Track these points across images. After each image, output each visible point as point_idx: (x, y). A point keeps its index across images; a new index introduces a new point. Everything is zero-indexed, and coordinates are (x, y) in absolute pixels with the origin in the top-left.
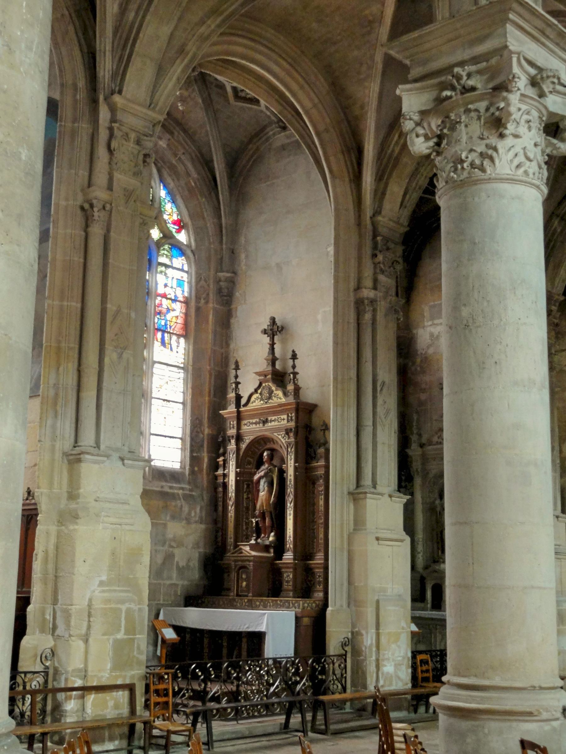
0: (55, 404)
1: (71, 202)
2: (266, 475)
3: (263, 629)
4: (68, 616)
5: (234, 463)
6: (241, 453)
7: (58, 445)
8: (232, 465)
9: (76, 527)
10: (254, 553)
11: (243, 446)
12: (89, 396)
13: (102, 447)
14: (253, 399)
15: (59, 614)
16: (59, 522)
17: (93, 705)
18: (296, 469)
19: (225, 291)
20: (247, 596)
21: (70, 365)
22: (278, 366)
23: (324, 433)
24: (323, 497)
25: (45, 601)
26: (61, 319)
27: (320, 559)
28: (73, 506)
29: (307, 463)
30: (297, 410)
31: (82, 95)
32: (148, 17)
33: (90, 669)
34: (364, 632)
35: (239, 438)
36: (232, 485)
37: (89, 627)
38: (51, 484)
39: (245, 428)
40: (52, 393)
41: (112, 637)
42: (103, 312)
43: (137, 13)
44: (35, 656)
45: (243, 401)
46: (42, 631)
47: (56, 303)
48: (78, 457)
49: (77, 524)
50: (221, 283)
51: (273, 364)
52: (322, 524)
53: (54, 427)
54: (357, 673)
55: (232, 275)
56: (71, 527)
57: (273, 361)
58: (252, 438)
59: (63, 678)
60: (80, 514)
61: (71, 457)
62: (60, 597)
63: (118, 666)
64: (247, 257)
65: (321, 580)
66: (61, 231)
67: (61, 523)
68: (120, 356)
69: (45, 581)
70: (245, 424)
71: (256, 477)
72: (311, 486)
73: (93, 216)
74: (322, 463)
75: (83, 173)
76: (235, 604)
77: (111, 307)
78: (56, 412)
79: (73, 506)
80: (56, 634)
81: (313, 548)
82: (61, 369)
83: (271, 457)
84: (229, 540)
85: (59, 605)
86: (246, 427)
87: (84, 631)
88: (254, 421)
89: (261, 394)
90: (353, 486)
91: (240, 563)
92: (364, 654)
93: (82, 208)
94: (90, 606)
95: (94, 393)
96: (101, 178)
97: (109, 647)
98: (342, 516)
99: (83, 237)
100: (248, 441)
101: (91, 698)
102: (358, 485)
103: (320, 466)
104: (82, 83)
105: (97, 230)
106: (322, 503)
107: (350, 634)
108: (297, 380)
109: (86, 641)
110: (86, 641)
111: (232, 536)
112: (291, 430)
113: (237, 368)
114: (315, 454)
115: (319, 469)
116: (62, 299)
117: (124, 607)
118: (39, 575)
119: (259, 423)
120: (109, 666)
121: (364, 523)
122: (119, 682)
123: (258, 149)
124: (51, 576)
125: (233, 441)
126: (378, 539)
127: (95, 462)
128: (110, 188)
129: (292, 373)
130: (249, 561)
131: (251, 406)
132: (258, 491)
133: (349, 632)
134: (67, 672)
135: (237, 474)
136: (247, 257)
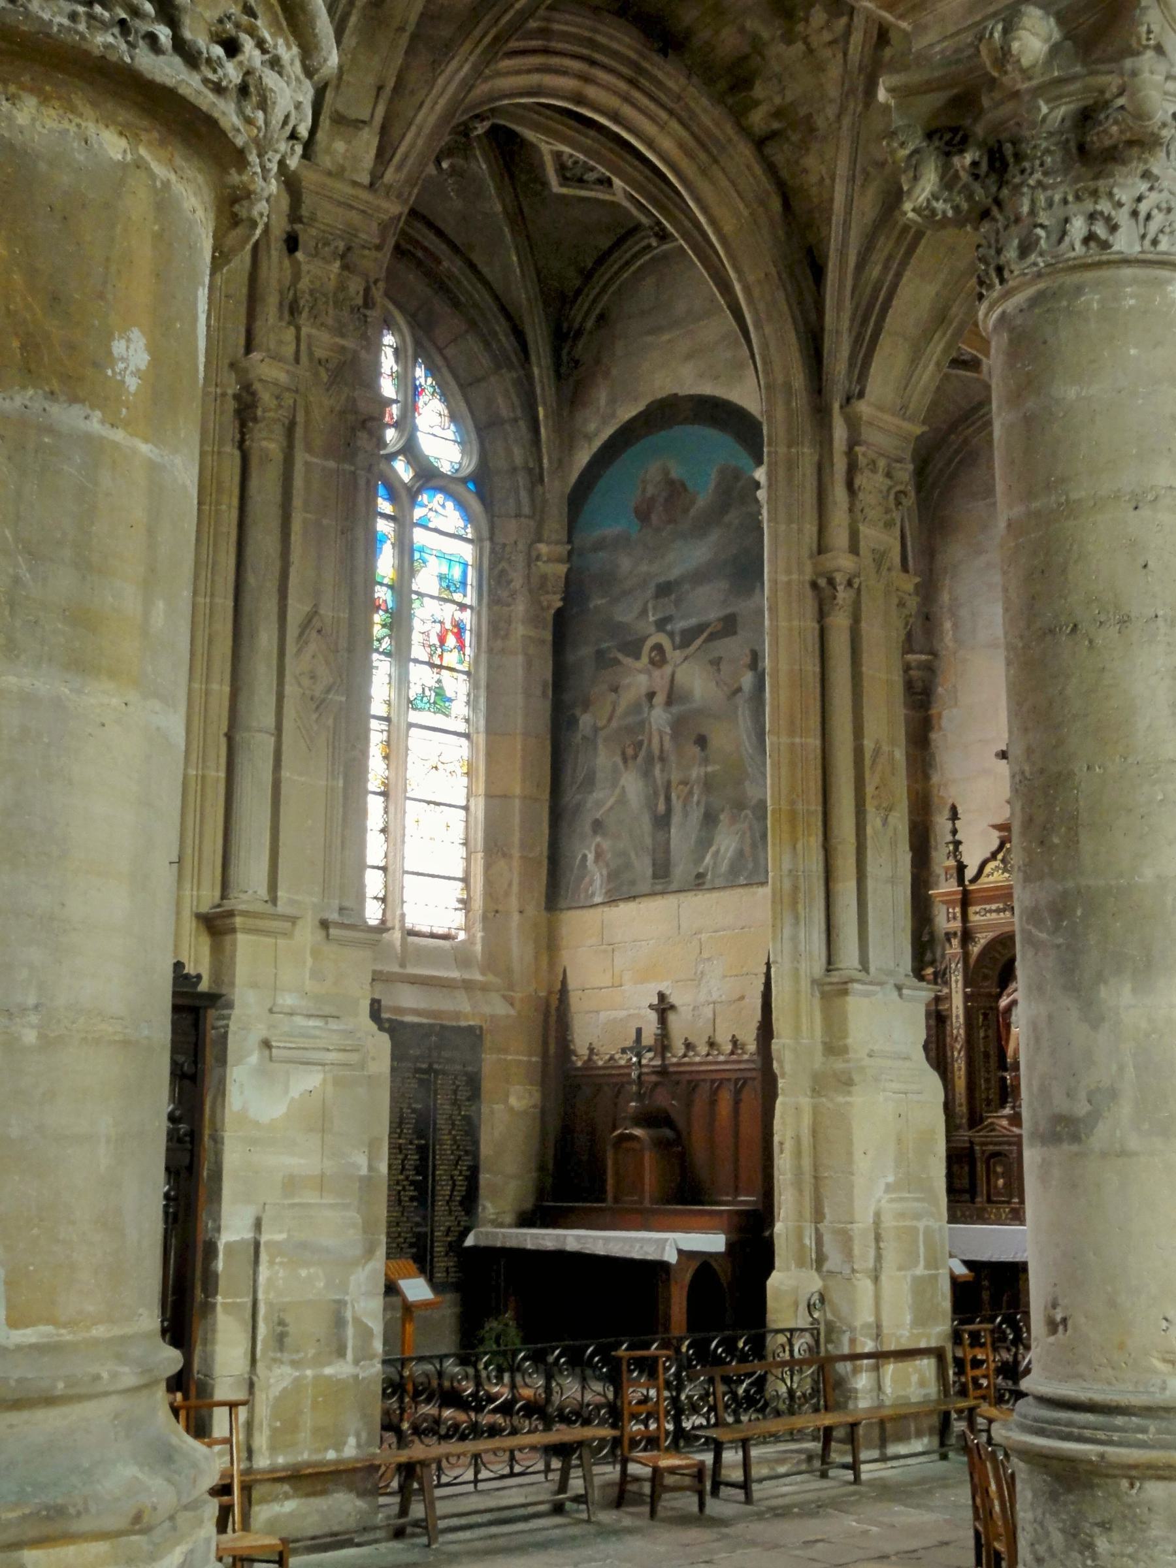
0: (794, 903)
1: (795, 577)
4: (846, 1240)
5: (960, 978)
6: (972, 960)
7: (803, 967)
8: (957, 982)
9: (848, 1099)
11: (975, 950)
12: (846, 890)
13: (872, 969)
15: (827, 1238)
16: (814, 1090)
17: (893, 1381)
19: (919, 685)
20: (1009, 1202)
21: (813, 839)
25: (800, 1215)
26: (792, 765)
28: (839, 1065)
31: (801, 402)
32: (908, 274)
33: (885, 1323)
35: (967, 936)
36: (957, 1017)
37: (879, 1258)
38: (797, 1029)
40: (787, 885)
41: (909, 1273)
42: (859, 752)
43: (886, 268)
44: (796, 1304)
45: (970, 873)
46: (801, 1264)
47: (785, 740)
48: (844, 986)
49: (849, 1093)
50: (912, 672)
53: (794, 939)
55: (930, 657)
56: (840, 1099)
58: (991, 935)
59: (845, 1339)
60: (856, 1078)
61: (827, 988)
62: (826, 1210)
63: (921, 1319)
64: (955, 626)
66: (783, 624)
67: (816, 1091)
68: (885, 822)
69: (798, 1183)
70: (976, 913)
73: (835, 598)
75: (811, 529)
76: (986, 1216)
77: (868, 744)
78: (797, 918)
79: (839, 1065)
80: (825, 1268)
82: (799, 846)
84: (958, 1109)
85: (826, 1223)
86: (977, 917)
87: (871, 1264)
88: (994, 907)
89: (1003, 861)
91: (991, 1147)
93: (814, 585)
94: (877, 1223)
95: (852, 885)
96: (839, 537)
97: (906, 1287)
99: (817, 633)
100: (983, 942)
101: (890, 1369)
104: (799, 381)
105: (840, 621)
109: (876, 1279)
110: (876, 1279)
111: (964, 1101)
113: (954, 815)
116: (792, 733)
117: (921, 1225)
118: (789, 1176)
119: (1004, 910)
120: (908, 1318)
122: (923, 1345)
123: (966, 441)
124: (808, 1178)
125: (955, 942)
127: (867, 995)
128: (854, 549)
130: (1010, 1144)
131: (986, 882)
134: (852, 1329)
135: (967, 997)
136: (955, 626)
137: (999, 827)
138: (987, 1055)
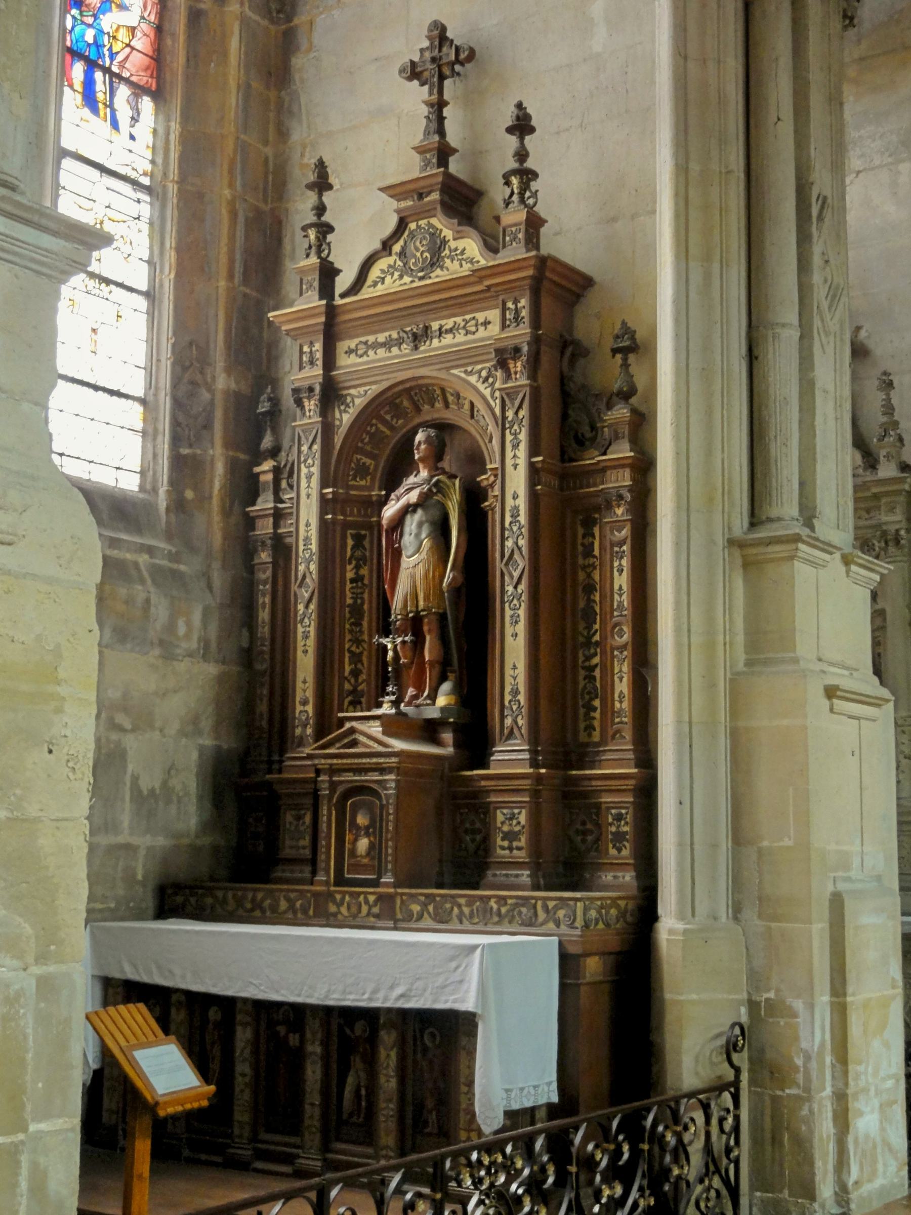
2: (423, 502)
3: (468, 1004)
5: (316, 470)
6: (338, 440)
8: (309, 477)
10: (399, 745)
11: (345, 418)
14: (375, 273)
18: (534, 471)
20: (375, 883)
22: (455, 166)
23: (625, 360)
24: (625, 562)
27: (619, 762)
29: (565, 456)
30: (536, 289)
34: (798, 1005)
36: (307, 539)
39: (346, 362)
45: (343, 282)
51: (443, 161)
52: (623, 647)
54: (776, 1140)
57: (444, 153)
58: (374, 389)
65: (626, 829)
70: (350, 352)
71: (389, 511)
72: (581, 531)
74: (622, 451)
76: (333, 908)
81: (590, 728)
83: (437, 454)
84: (299, 708)
86: (353, 359)
88: (381, 338)
89: (402, 254)
90: (740, 523)
91: (349, 777)
92: (800, 1078)
98: (710, 620)
100: (360, 402)
102: (755, 520)
103: (619, 464)
106: (622, 580)
107: (743, 1010)
108: (535, 195)
111: (310, 694)
112: (517, 350)
113: (322, 184)
114: (593, 428)
115: (612, 475)
119: (399, 342)
121: (787, 639)
125: (311, 405)
126: (831, 692)
129: (514, 172)
130: (382, 770)
132: (397, 554)
133: (740, 1003)
135: (325, 504)
137: (394, 191)
138: (357, 611)
